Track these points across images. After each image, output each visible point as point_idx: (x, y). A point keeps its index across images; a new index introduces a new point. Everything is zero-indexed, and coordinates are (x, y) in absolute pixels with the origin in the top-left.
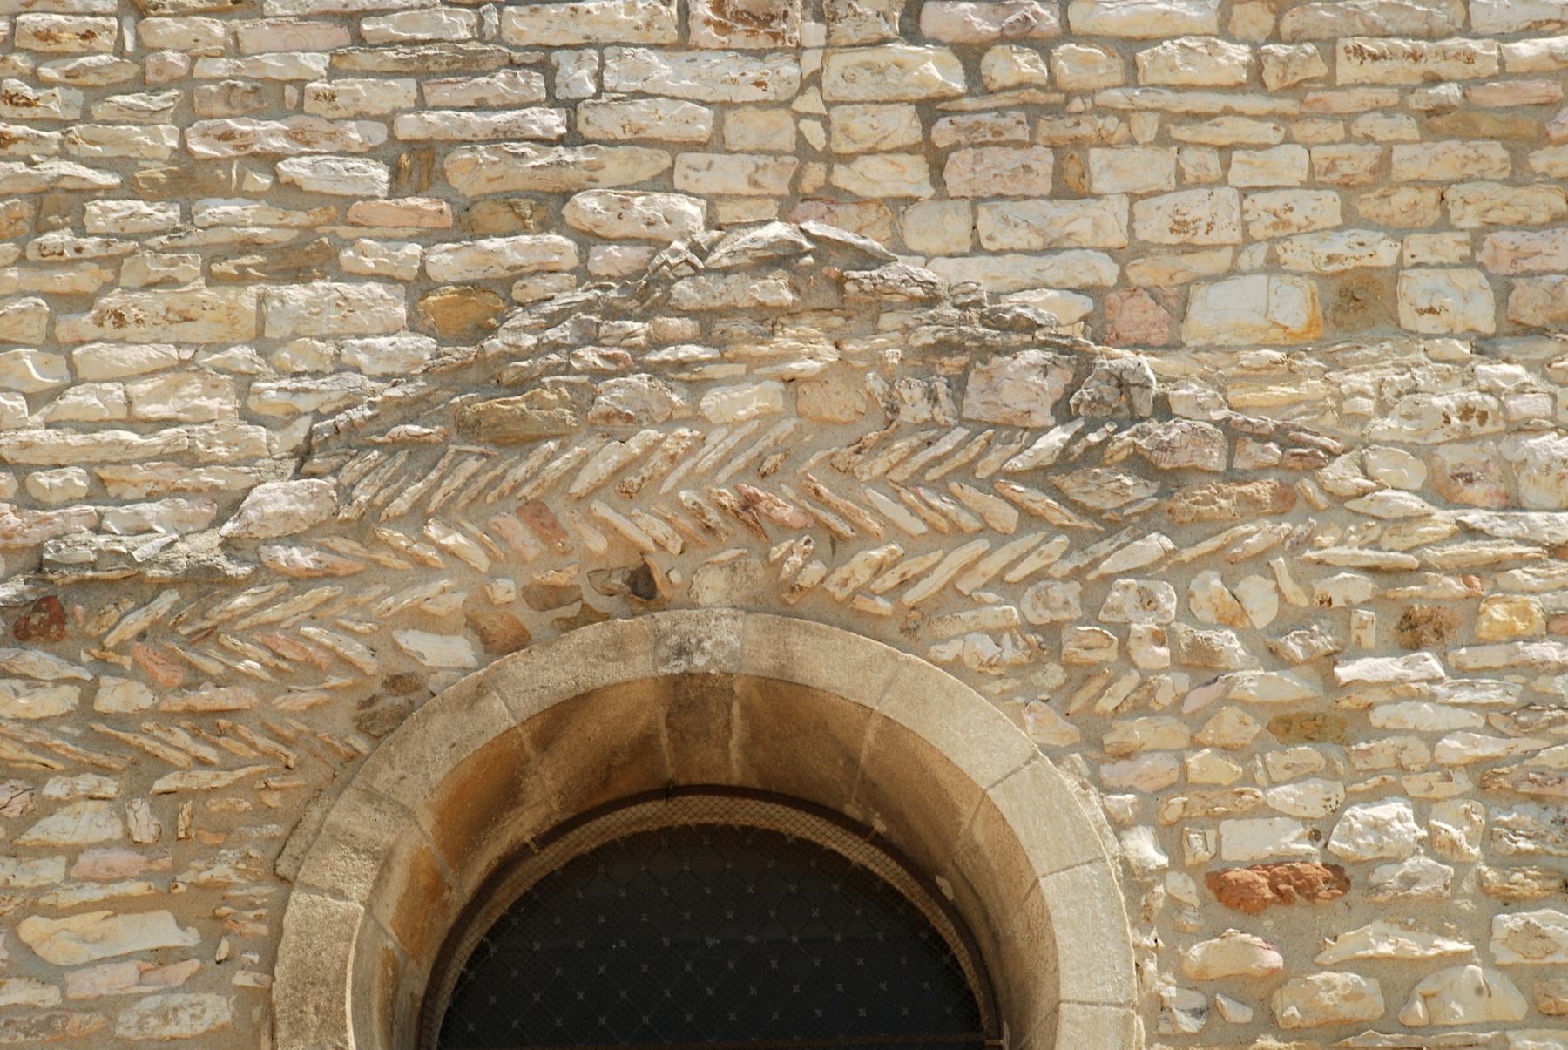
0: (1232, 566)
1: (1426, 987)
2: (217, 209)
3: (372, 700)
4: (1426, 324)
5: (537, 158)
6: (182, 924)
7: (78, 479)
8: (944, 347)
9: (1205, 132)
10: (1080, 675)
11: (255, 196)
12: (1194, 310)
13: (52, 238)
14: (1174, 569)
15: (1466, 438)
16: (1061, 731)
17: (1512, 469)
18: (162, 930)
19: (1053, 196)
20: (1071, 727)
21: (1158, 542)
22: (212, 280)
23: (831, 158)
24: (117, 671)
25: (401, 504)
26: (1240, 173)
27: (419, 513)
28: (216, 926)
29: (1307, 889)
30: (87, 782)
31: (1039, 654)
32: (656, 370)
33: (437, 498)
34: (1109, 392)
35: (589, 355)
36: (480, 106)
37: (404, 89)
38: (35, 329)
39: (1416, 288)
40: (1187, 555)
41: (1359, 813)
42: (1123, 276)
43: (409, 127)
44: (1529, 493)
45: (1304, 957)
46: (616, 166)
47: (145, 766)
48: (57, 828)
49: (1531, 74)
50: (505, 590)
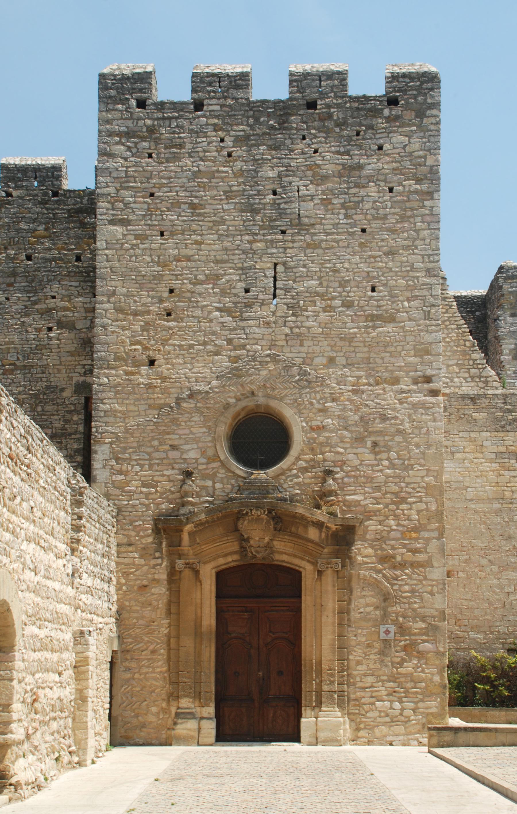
0: (316, 392)
2: (209, 347)
5: (243, 341)
7: (194, 379)
8: (286, 366)
9: (317, 339)
13: (191, 351)
14: (309, 393)
16: (296, 411)
17: (346, 381)
18: (204, 430)
22: (208, 356)
23: (275, 341)
26: (320, 344)
27: (229, 385)
28: (210, 429)
29: (320, 428)
32: (255, 369)
35: (248, 367)
36: (236, 334)
37: (228, 332)
38: (189, 362)
39: (338, 359)
41: (326, 420)
43: (229, 337)
44: (347, 384)
45: (319, 436)
46: (252, 342)
48: (193, 419)
49: (352, 334)
50: (238, 394)
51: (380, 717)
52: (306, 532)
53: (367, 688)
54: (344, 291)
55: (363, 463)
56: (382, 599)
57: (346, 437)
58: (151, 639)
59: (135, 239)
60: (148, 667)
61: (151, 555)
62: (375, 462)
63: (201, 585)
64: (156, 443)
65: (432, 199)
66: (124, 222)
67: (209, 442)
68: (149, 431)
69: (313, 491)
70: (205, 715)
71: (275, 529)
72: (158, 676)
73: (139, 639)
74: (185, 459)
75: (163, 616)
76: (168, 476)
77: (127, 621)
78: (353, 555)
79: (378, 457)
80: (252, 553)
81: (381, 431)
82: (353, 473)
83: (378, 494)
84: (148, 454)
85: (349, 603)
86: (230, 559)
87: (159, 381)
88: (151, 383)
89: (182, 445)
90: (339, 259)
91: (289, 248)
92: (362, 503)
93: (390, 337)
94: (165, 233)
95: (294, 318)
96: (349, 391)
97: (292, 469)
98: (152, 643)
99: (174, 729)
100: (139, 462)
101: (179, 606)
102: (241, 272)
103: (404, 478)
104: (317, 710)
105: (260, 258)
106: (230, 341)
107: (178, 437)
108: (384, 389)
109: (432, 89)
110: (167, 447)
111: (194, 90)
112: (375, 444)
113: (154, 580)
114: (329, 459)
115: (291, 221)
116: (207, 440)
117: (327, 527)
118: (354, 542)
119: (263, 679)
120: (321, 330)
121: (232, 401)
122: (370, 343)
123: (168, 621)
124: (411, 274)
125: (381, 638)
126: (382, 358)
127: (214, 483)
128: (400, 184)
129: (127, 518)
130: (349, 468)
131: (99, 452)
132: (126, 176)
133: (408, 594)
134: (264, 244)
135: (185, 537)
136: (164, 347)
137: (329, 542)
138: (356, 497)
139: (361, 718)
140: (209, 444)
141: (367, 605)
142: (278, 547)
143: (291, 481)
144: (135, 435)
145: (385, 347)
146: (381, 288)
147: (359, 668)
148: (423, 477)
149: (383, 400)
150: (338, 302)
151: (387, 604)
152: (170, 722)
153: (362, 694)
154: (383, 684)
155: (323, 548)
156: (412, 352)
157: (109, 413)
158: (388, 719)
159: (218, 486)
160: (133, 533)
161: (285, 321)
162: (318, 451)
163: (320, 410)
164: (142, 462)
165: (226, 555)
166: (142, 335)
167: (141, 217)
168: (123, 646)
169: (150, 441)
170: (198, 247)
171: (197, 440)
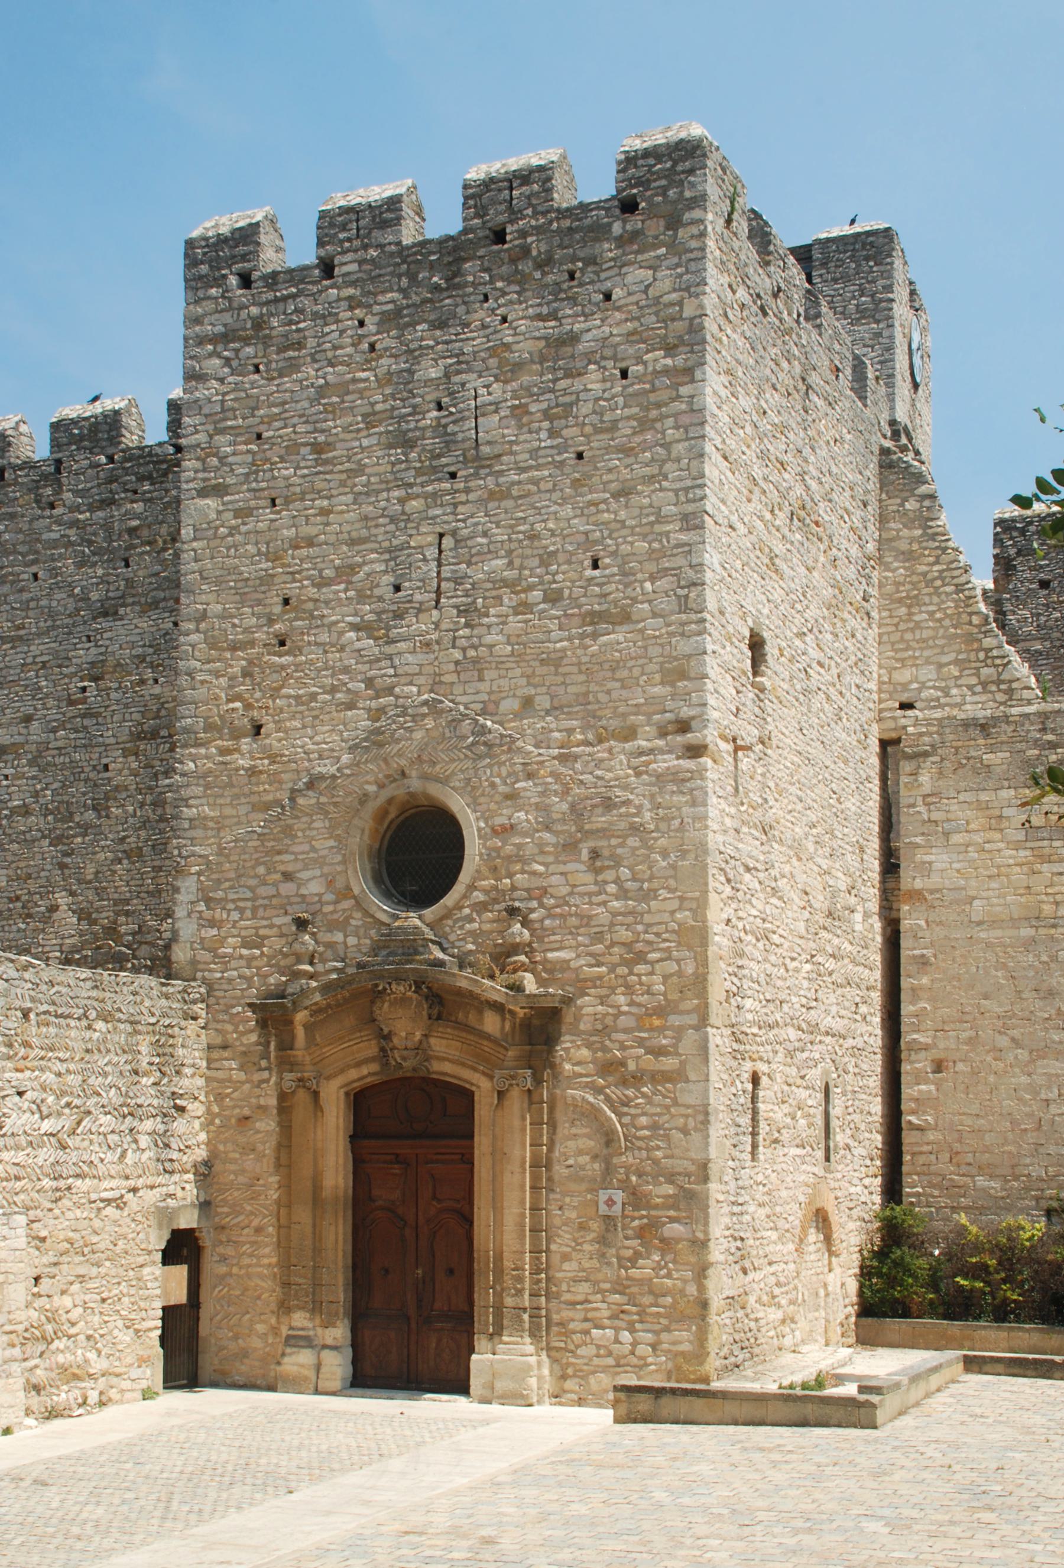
0: (501, 764)
2: (339, 695)
7: (316, 755)
8: (453, 720)
10: (474, 788)
14: (490, 766)
16: (469, 800)
18: (332, 843)
23: (440, 675)
28: (340, 842)
31: (468, 784)
35: (394, 726)
39: (538, 699)
45: (505, 843)
46: (403, 680)
47: (327, 813)
50: (380, 776)
51: (598, 1356)
52: (481, 1020)
54: (547, 573)
55: (576, 890)
56: (603, 1141)
57: (548, 844)
59: (235, 518)
60: (251, 1255)
62: (593, 888)
64: (261, 870)
65: (693, 381)
66: (219, 491)
67: (339, 863)
68: (252, 850)
69: (496, 945)
70: (329, 1341)
74: (303, 896)
75: (272, 1170)
76: (279, 927)
78: (558, 1061)
79: (600, 878)
81: (604, 830)
84: (252, 889)
87: (266, 762)
88: (255, 766)
89: (299, 871)
90: (540, 514)
91: (462, 503)
92: (573, 964)
93: (620, 651)
94: (277, 501)
95: (467, 631)
96: (554, 758)
97: (463, 907)
101: (290, 1153)
102: (387, 556)
103: (642, 914)
105: (417, 528)
106: (369, 682)
107: (292, 857)
108: (610, 750)
109: (691, 171)
110: (278, 876)
111: (321, 244)
112: (595, 854)
113: (260, 1107)
114: (519, 885)
115: (464, 455)
117: (510, 1011)
120: (509, 648)
121: (372, 788)
124: (658, 528)
126: (609, 692)
128: (639, 360)
129: (221, 1001)
130: (552, 901)
131: (183, 890)
132: (223, 411)
133: (647, 1133)
134: (422, 501)
135: (300, 1033)
136: (274, 701)
137: (517, 1038)
140: (339, 868)
141: (580, 1152)
143: (461, 928)
144: (232, 858)
145: (613, 670)
146: (607, 561)
147: (566, 1266)
148: (673, 912)
149: (609, 770)
150: (537, 595)
151: (611, 1150)
153: (571, 1314)
154: (604, 1297)
155: (506, 1049)
156: (657, 677)
157: (197, 823)
158: (610, 1361)
160: (229, 1028)
161: (455, 638)
162: (503, 872)
163: (508, 797)
164: (241, 904)
165: (359, 1064)
166: (243, 684)
167: (242, 479)
168: (217, 1219)
169: (253, 868)
170: (323, 519)
171: (320, 862)
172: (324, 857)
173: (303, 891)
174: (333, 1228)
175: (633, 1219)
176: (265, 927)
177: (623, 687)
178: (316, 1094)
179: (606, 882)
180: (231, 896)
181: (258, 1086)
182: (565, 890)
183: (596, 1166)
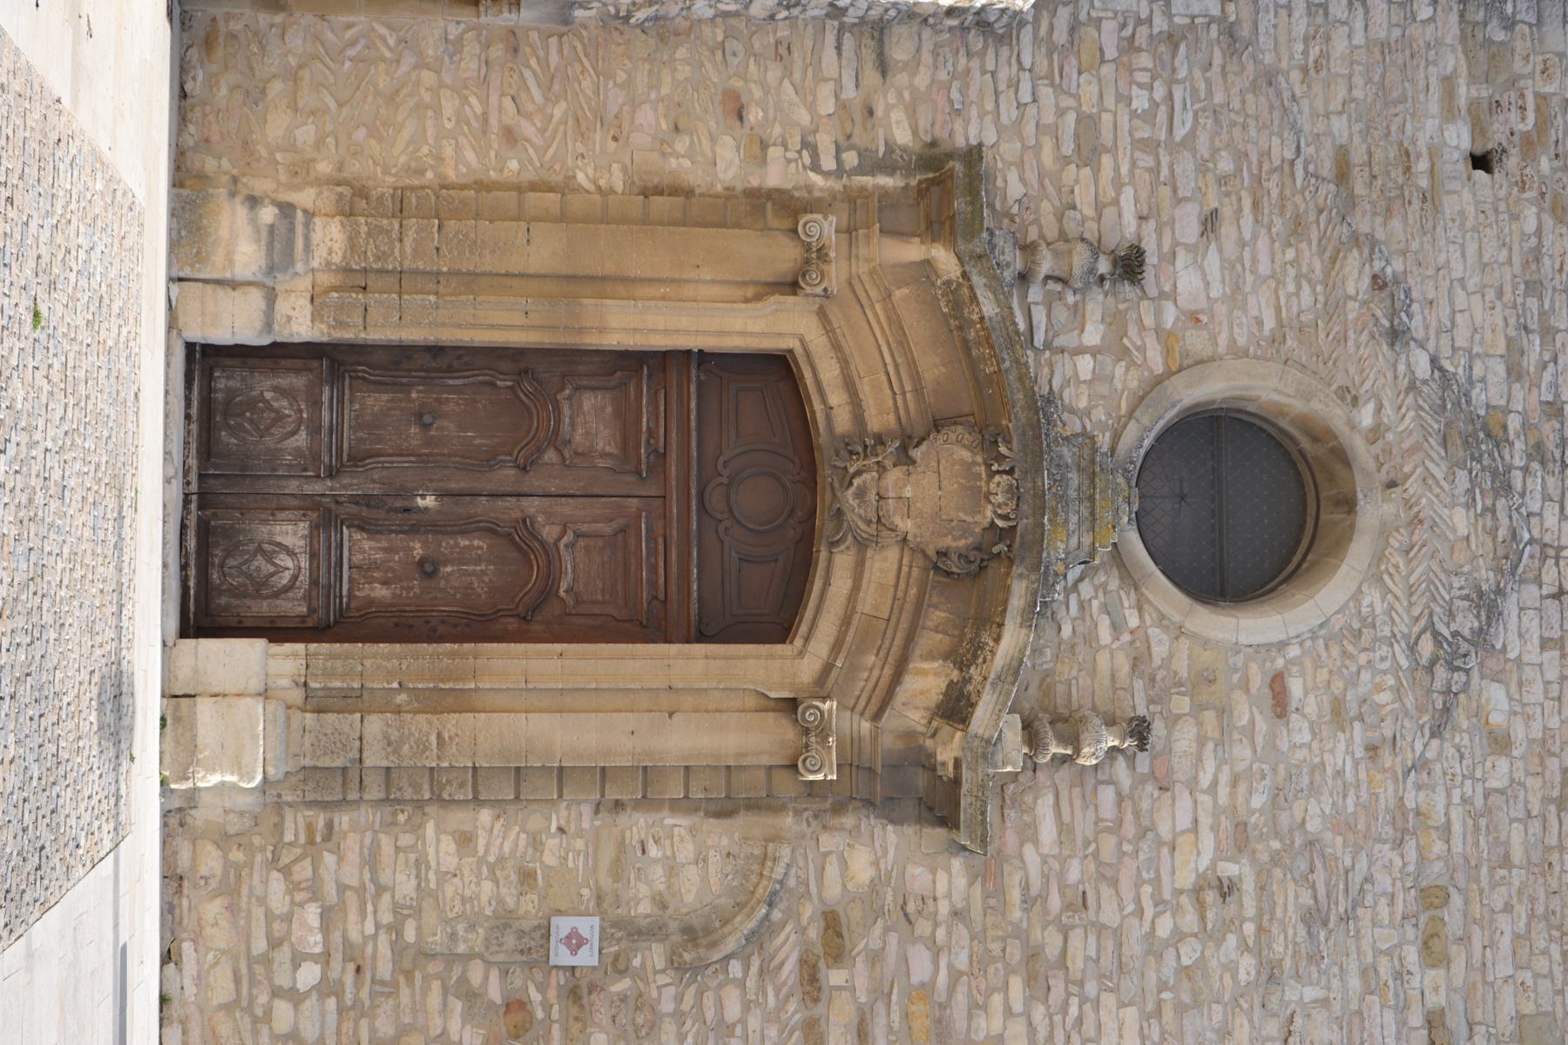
0: (1398, 690)
1: (1244, 740)
3: (1349, 392)
4: (1488, 764)
6: (1272, 330)
11: (1541, 354)
12: (1496, 684)
15: (1445, 774)
18: (1270, 324)
19: (1541, 637)
20: (1337, 630)
21: (1404, 663)
24: (1361, 308)
25: (1421, 402)
26: (1548, 704)
30: (1321, 298)
33: (1423, 414)
34: (1462, 651)
39: (1503, 764)
40: (1401, 674)
42: (1509, 660)
44: (1422, 794)
48: (1306, 289)
51: (269, 916)
53: (374, 872)
55: (1165, 851)
56: (696, 922)
58: (556, 131)
60: (460, 118)
61: (849, 137)
63: (747, 301)
64: (1225, 165)
67: (1233, 341)
70: (282, 307)
71: (942, 554)
72: (425, 150)
73: (556, 87)
76: (1116, 202)
77: (621, 49)
79: (1184, 900)
80: (858, 473)
82: (1129, 817)
83: (1055, 902)
85: (683, 805)
86: (837, 398)
89: (1220, 250)
92: (1029, 849)
98: (542, 131)
99: (232, 194)
100: (1163, 109)
103: (1115, 990)
104: (297, 696)
107: (1247, 236)
112: (1227, 890)
113: (764, 146)
116: (1236, 330)
118: (892, 821)
119: (407, 510)
122: (1557, 869)
123: (619, 186)
125: (555, 921)
127: (1094, 352)
129: (975, 64)
133: (710, 1015)
135: (913, 251)
138: (1048, 831)
139: (263, 849)
141: (672, 869)
142: (877, 565)
147: (448, 844)
152: (261, 186)
153: (353, 857)
156: (1529, 1008)
157: (1320, 19)
158: (260, 945)
159: (1085, 365)
160: (922, 79)
165: (850, 386)
168: (534, 35)
171: (1236, 297)
172: (1244, 308)
173: (1182, 258)
174: (519, 319)
175: (542, 989)
176: (1117, 169)
177: (1517, 937)
178: (792, 286)
179: (1177, 910)
180: (1178, 93)
181: (805, 144)
182: (1164, 829)
183: (645, 908)
